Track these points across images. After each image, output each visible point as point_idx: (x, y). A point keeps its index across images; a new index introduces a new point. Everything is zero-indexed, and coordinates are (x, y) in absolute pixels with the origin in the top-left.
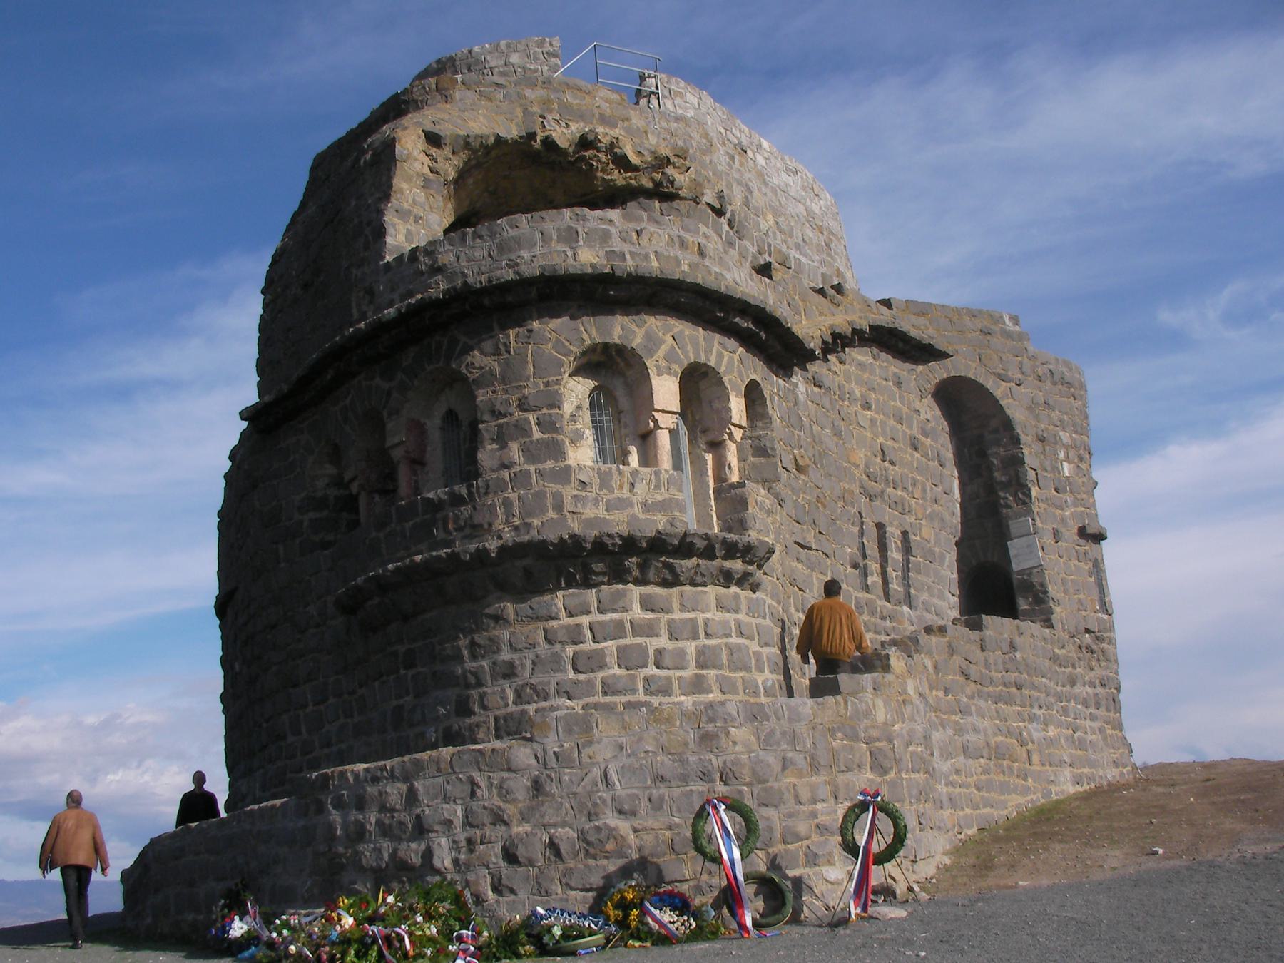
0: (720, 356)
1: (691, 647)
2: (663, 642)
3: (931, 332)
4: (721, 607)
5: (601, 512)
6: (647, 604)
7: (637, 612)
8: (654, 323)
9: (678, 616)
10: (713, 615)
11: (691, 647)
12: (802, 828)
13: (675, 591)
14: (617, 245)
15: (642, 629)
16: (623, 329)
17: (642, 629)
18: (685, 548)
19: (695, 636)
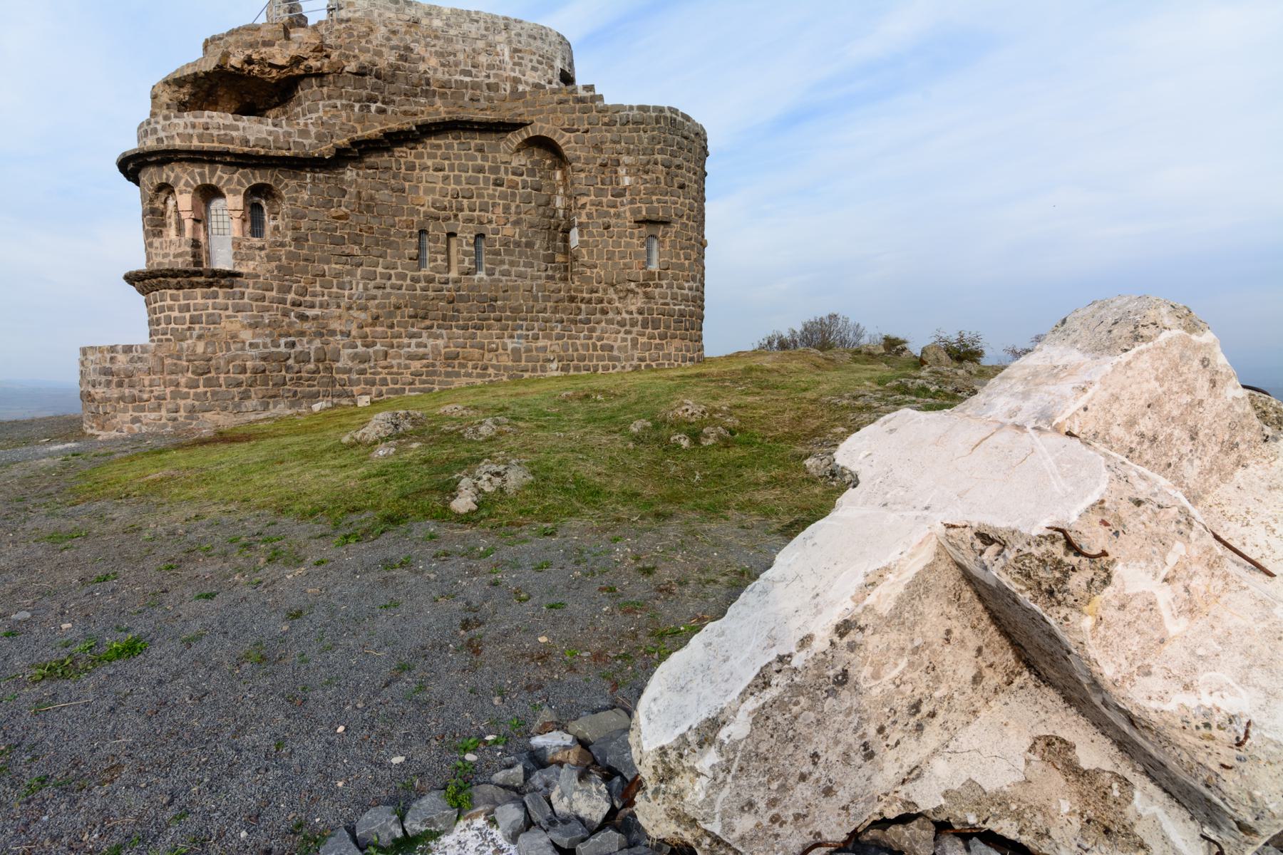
0: (221, 178)
1: (187, 315)
2: (176, 314)
3: (522, 110)
4: (203, 297)
5: (159, 259)
6: (173, 298)
7: (169, 302)
8: (178, 168)
9: (182, 302)
10: (200, 301)
11: (187, 315)
12: (145, 396)
13: (181, 292)
14: (162, 134)
15: (171, 308)
16: (169, 173)
17: (171, 308)
18: (174, 274)
19: (189, 310)
